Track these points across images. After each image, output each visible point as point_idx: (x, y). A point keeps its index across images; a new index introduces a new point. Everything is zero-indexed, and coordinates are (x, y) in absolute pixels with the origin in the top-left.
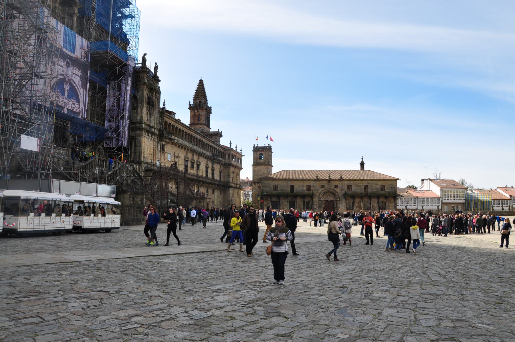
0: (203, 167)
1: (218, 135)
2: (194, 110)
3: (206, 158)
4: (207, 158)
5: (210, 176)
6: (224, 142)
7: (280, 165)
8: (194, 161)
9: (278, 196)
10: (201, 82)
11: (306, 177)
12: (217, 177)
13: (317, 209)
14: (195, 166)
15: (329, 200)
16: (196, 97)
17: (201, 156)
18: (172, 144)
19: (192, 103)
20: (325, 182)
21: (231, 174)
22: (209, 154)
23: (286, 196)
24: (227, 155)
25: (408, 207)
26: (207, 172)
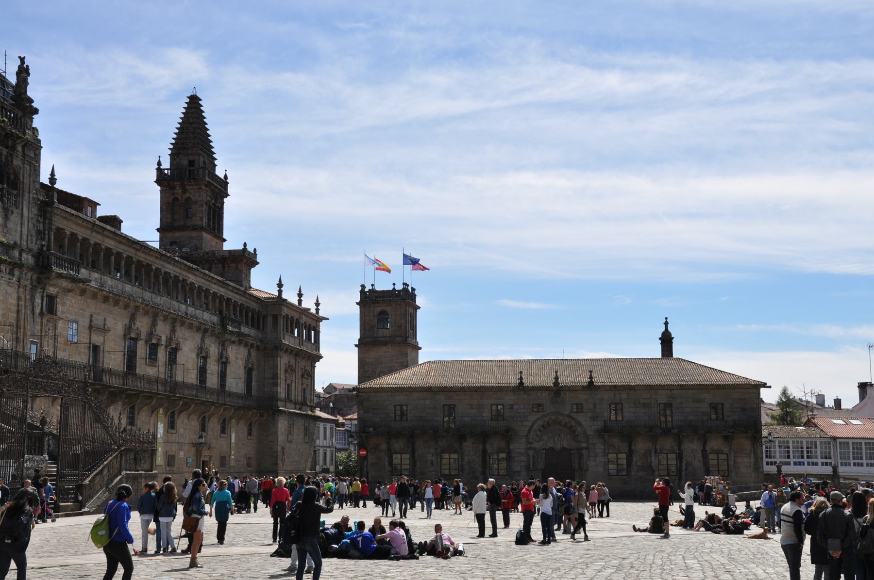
0: (187, 356)
1: (245, 260)
2: (173, 188)
3: (198, 329)
4: (203, 330)
5: (212, 381)
6: (261, 282)
7: (445, 343)
8: (159, 339)
10: (194, 104)
11: (490, 380)
12: (235, 383)
14: (162, 355)
15: (558, 447)
16: (179, 148)
17: (182, 324)
18: (83, 292)
19: (166, 165)
20: (545, 394)
21: (282, 375)
22: (208, 317)
24: (270, 320)
25: (785, 469)
26: (202, 372)
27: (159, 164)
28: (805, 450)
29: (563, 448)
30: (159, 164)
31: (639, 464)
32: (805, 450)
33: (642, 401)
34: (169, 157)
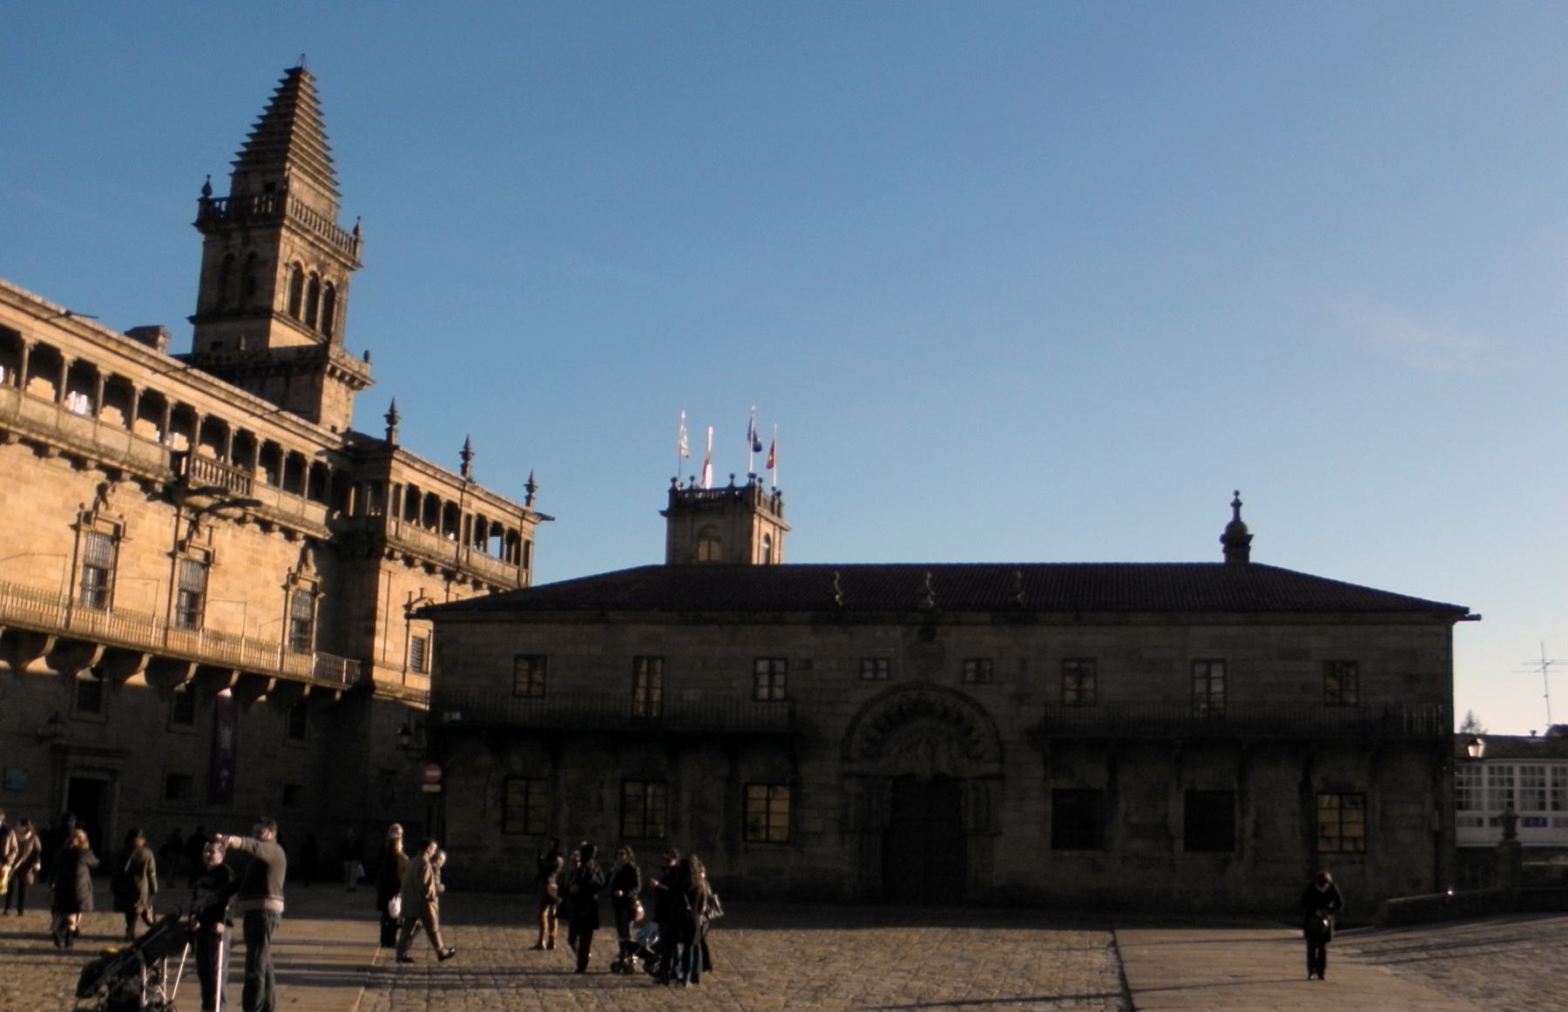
2: (226, 235)
19: (222, 188)
27: (207, 189)
28: (1549, 788)
30: (207, 189)
31: (1134, 819)
32: (1549, 788)
34: (229, 179)
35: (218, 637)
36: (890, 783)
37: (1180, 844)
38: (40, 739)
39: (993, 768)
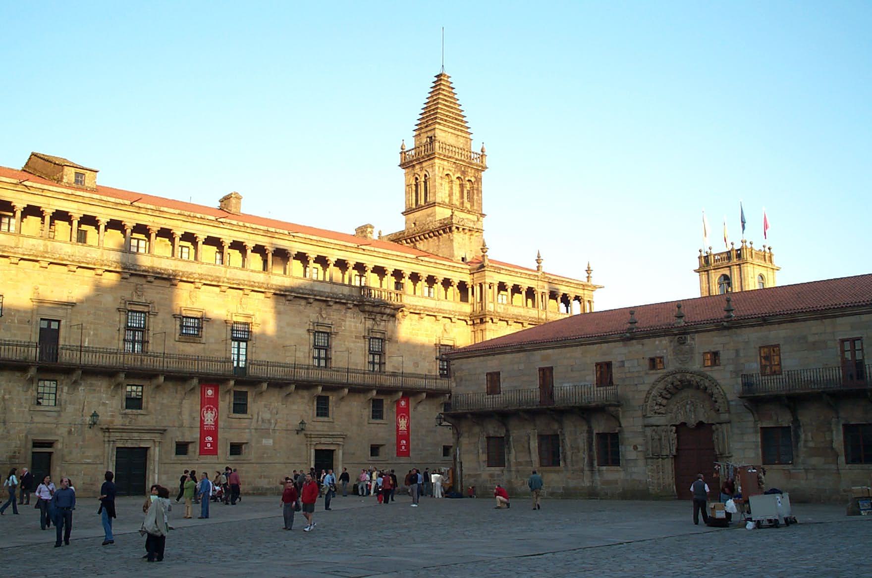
9: (503, 416)
13: (641, 462)
15: (692, 421)
19: (410, 144)
20: (665, 341)
23: (530, 414)
29: (700, 424)
31: (811, 444)
33: (811, 339)
35: (394, 375)
36: (674, 428)
37: (842, 459)
38: (298, 432)
39: (725, 417)
